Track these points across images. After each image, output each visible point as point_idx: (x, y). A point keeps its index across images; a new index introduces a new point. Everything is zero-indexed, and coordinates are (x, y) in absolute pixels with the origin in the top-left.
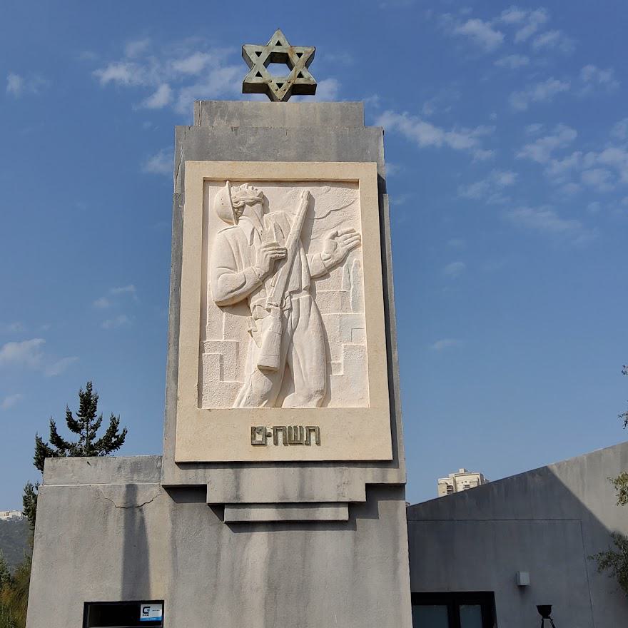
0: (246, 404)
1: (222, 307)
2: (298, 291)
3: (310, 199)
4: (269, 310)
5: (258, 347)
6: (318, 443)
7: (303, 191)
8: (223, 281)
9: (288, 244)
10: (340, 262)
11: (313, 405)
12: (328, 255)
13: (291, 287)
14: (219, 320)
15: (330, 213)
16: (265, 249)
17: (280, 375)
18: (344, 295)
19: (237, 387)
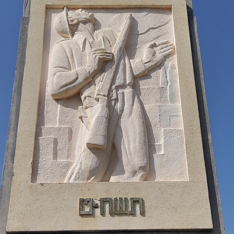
0: (77, 178)
1: (57, 100)
2: (123, 86)
3: (132, 19)
4: (98, 100)
5: (88, 123)
6: (143, 213)
7: (125, 17)
8: (58, 77)
9: (115, 50)
10: (159, 65)
11: (137, 179)
12: (147, 60)
13: (118, 82)
14: (54, 110)
15: (149, 30)
16: (94, 52)
17: (107, 154)
18: (162, 89)
19: (68, 165)
